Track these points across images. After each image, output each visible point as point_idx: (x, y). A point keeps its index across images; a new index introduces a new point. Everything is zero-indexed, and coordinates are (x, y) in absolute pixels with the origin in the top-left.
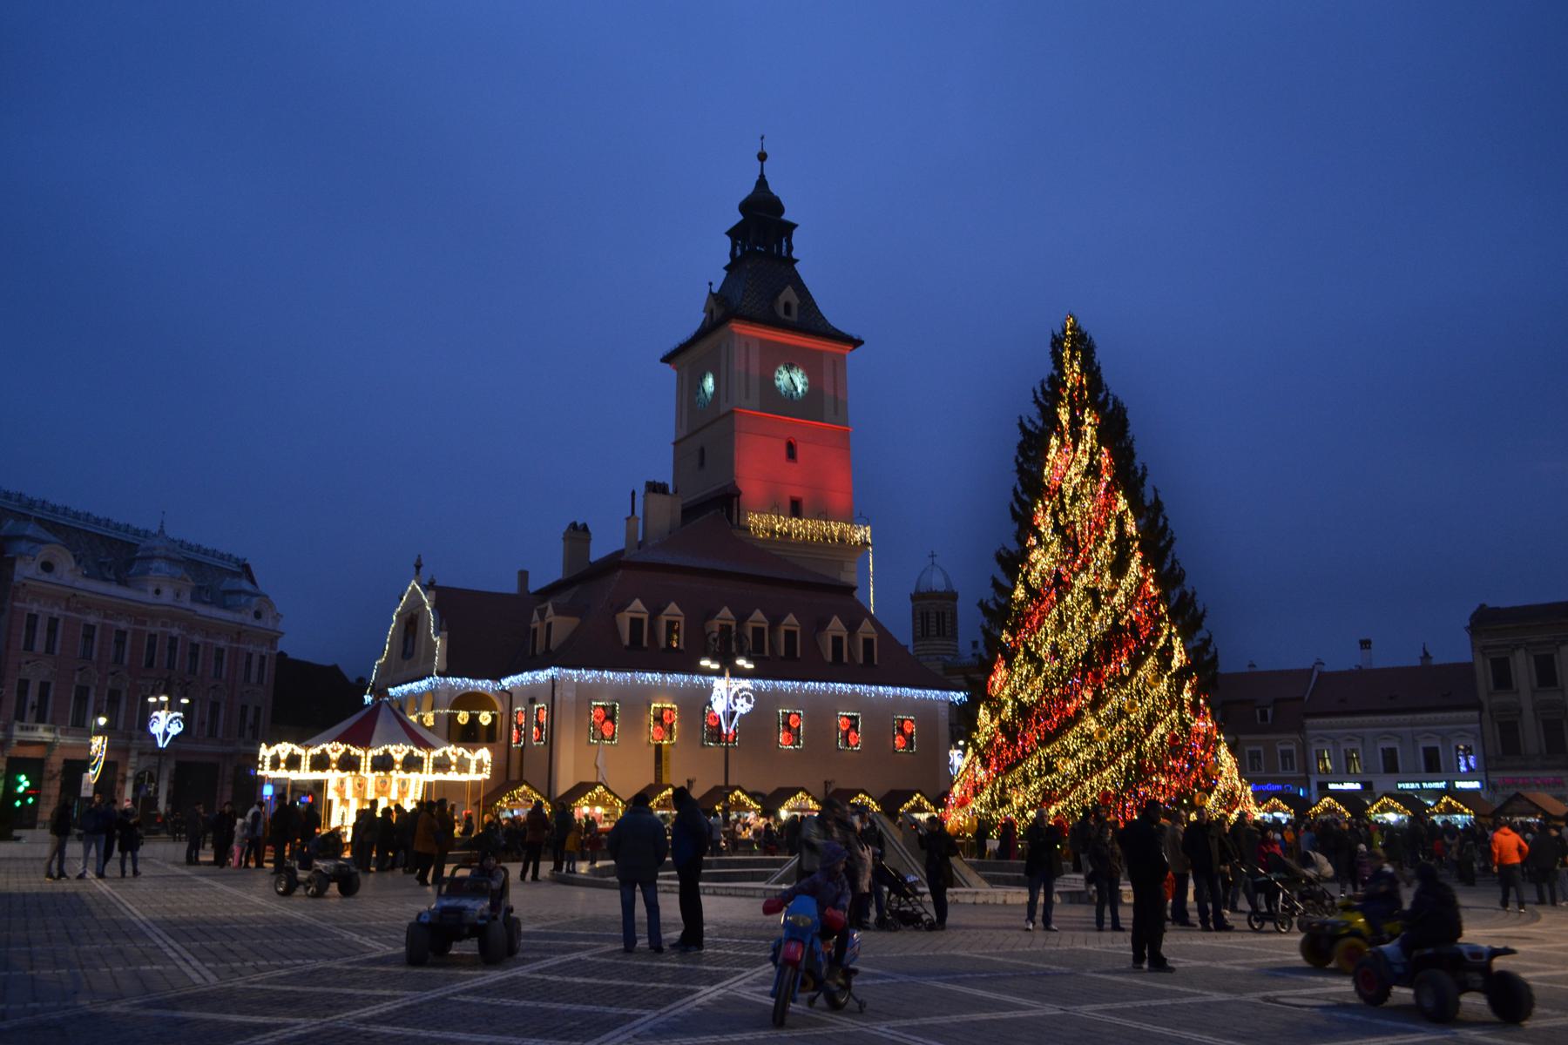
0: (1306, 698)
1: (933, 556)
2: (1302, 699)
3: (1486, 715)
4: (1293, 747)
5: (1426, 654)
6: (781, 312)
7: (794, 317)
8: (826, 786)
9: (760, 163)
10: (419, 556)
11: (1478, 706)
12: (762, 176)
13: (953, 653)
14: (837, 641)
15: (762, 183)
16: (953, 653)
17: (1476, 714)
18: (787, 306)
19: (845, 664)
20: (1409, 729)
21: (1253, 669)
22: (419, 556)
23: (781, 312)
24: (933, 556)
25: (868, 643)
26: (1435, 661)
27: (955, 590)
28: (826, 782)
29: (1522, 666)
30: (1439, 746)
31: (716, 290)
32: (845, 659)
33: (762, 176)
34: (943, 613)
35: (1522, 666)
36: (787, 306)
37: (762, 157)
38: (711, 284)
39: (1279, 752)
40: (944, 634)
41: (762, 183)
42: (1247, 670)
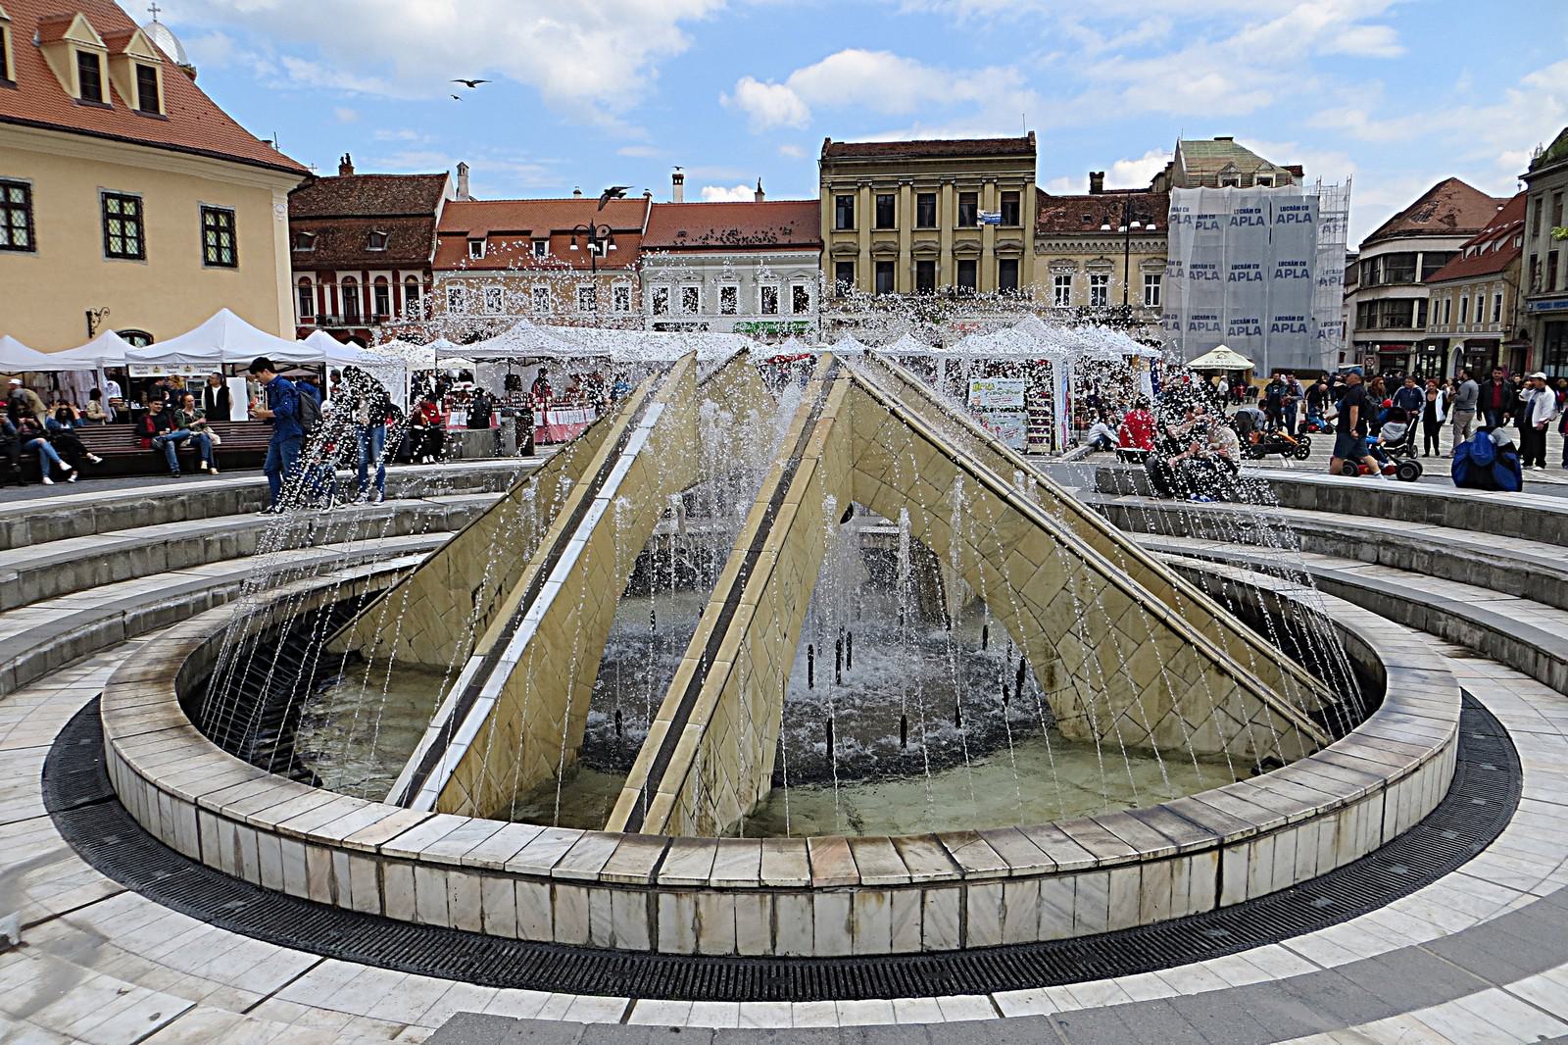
0: (644, 231)
1: (154, 10)
2: (640, 231)
3: (826, 255)
5: (760, 189)
8: (90, 320)
11: (821, 246)
14: (88, 61)
17: (818, 253)
19: (108, 107)
20: (751, 267)
21: (578, 197)
24: (154, 10)
25: (146, 74)
26: (766, 199)
28: (89, 314)
29: (865, 207)
30: (738, 287)
32: (106, 98)
35: (865, 207)
42: (572, 196)
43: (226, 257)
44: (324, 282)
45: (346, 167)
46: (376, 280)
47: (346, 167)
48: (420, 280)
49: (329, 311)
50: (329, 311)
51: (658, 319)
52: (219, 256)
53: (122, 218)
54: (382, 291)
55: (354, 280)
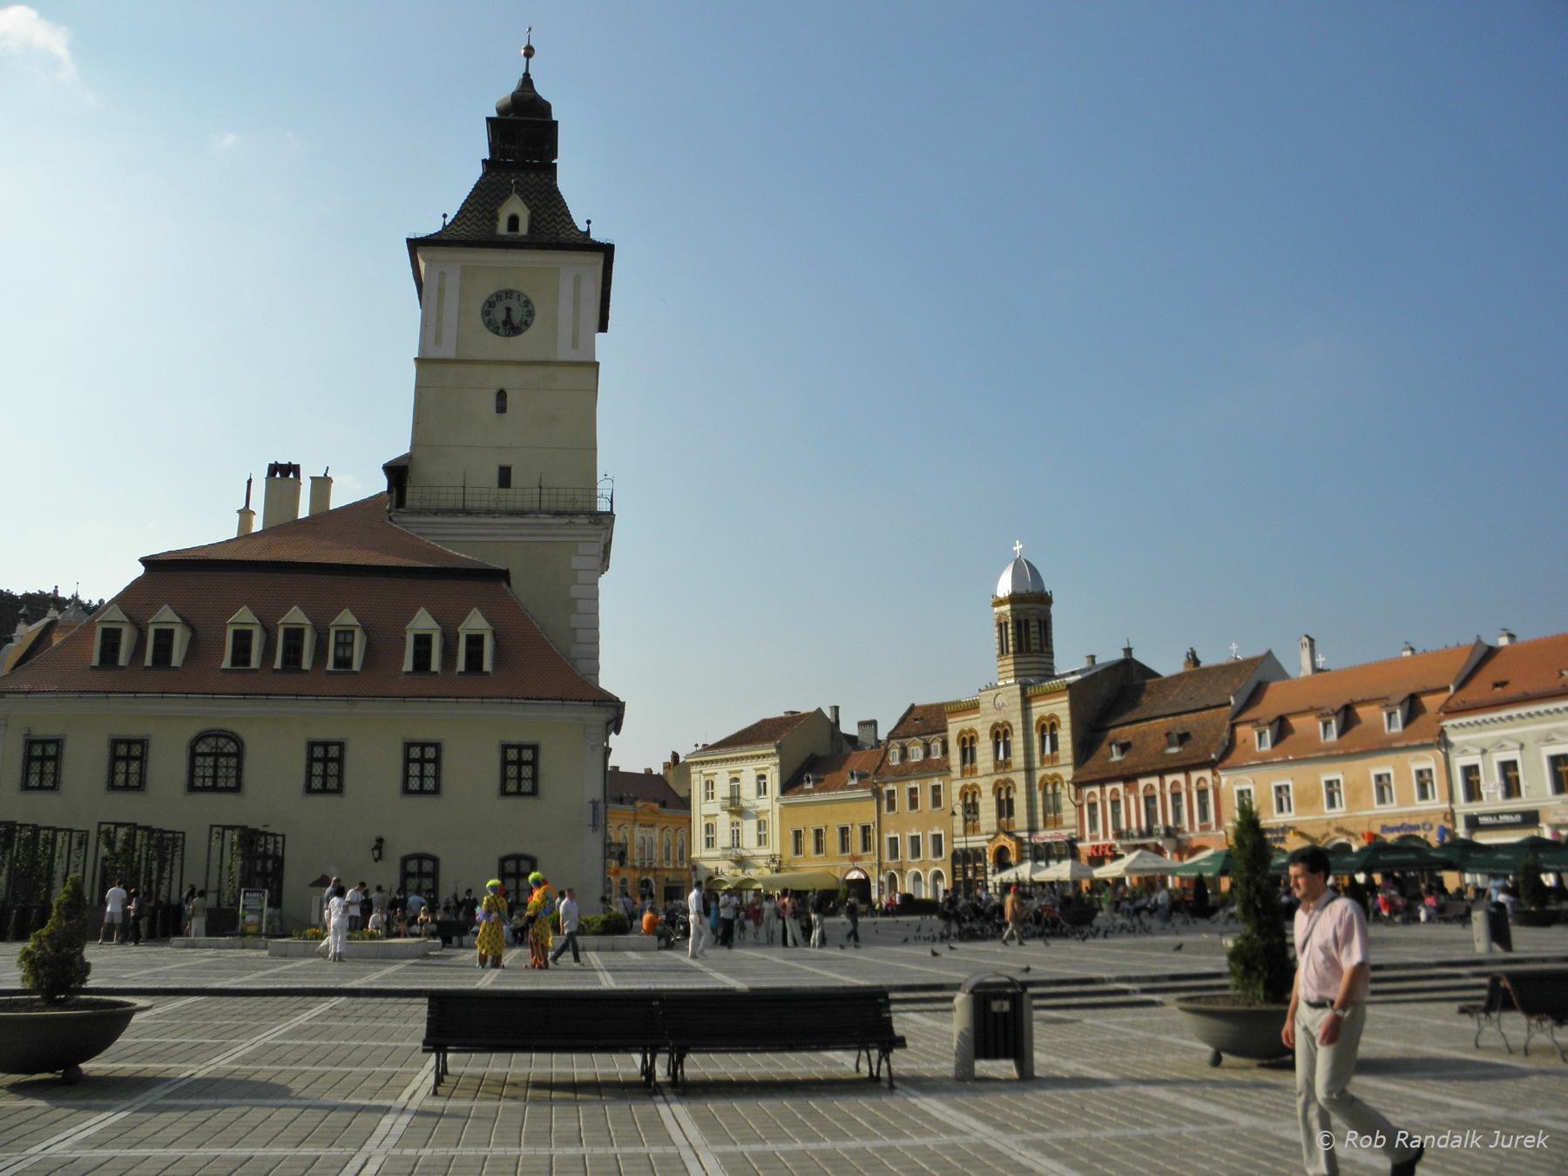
2: (1446, 689)
4: (1431, 765)
6: (502, 228)
7: (523, 228)
9: (525, 59)
10: (56, 587)
12: (527, 76)
13: (1043, 672)
15: (527, 80)
16: (1043, 672)
18: (513, 222)
22: (56, 587)
23: (502, 228)
27: (1047, 590)
31: (448, 221)
33: (527, 76)
34: (1027, 622)
36: (513, 222)
37: (529, 51)
38: (445, 216)
39: (1414, 774)
40: (1028, 650)
41: (527, 80)
43: (527, 787)
44: (1130, 792)
45: (1194, 660)
46: (1146, 788)
47: (1194, 660)
48: (1210, 782)
49: (1134, 824)
50: (1134, 824)
51: (1474, 808)
52: (519, 786)
53: (422, 761)
54: (1176, 797)
55: (1152, 787)
